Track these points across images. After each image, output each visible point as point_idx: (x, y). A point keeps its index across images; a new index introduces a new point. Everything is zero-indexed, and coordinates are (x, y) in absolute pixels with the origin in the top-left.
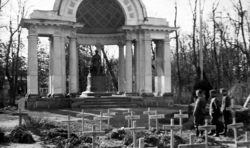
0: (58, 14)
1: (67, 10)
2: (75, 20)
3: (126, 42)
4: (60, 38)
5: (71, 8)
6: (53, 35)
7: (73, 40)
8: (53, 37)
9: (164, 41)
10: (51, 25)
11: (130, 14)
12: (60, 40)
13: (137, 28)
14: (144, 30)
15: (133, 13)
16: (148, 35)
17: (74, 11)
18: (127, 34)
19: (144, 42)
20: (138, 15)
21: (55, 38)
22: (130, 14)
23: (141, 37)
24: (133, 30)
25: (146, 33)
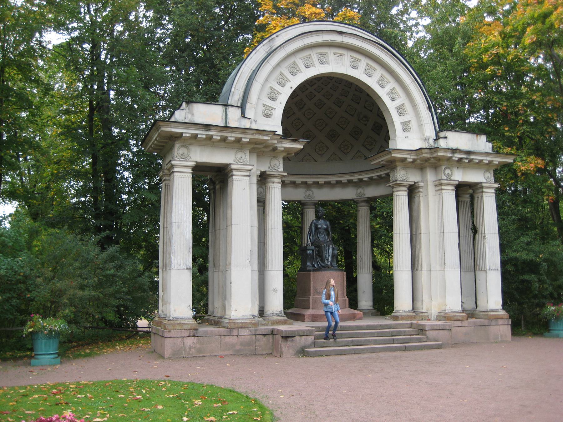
0: (243, 115)
1: (261, 109)
2: (280, 131)
3: (395, 189)
4: (248, 174)
5: (270, 103)
6: (233, 166)
7: (276, 180)
8: (231, 170)
9: (482, 187)
10: (229, 138)
11: (402, 123)
12: (248, 178)
13: (426, 155)
14: (439, 159)
15: (409, 122)
16: (448, 171)
17: (277, 110)
18: (398, 168)
19: (439, 188)
20: (420, 126)
21: (235, 173)
22: (402, 123)
23: (430, 177)
24: (414, 161)
25: (443, 168)
